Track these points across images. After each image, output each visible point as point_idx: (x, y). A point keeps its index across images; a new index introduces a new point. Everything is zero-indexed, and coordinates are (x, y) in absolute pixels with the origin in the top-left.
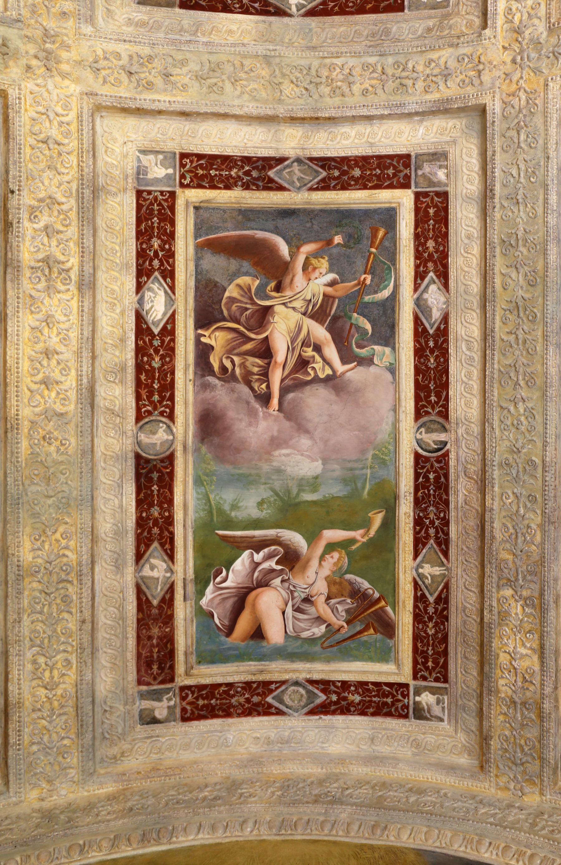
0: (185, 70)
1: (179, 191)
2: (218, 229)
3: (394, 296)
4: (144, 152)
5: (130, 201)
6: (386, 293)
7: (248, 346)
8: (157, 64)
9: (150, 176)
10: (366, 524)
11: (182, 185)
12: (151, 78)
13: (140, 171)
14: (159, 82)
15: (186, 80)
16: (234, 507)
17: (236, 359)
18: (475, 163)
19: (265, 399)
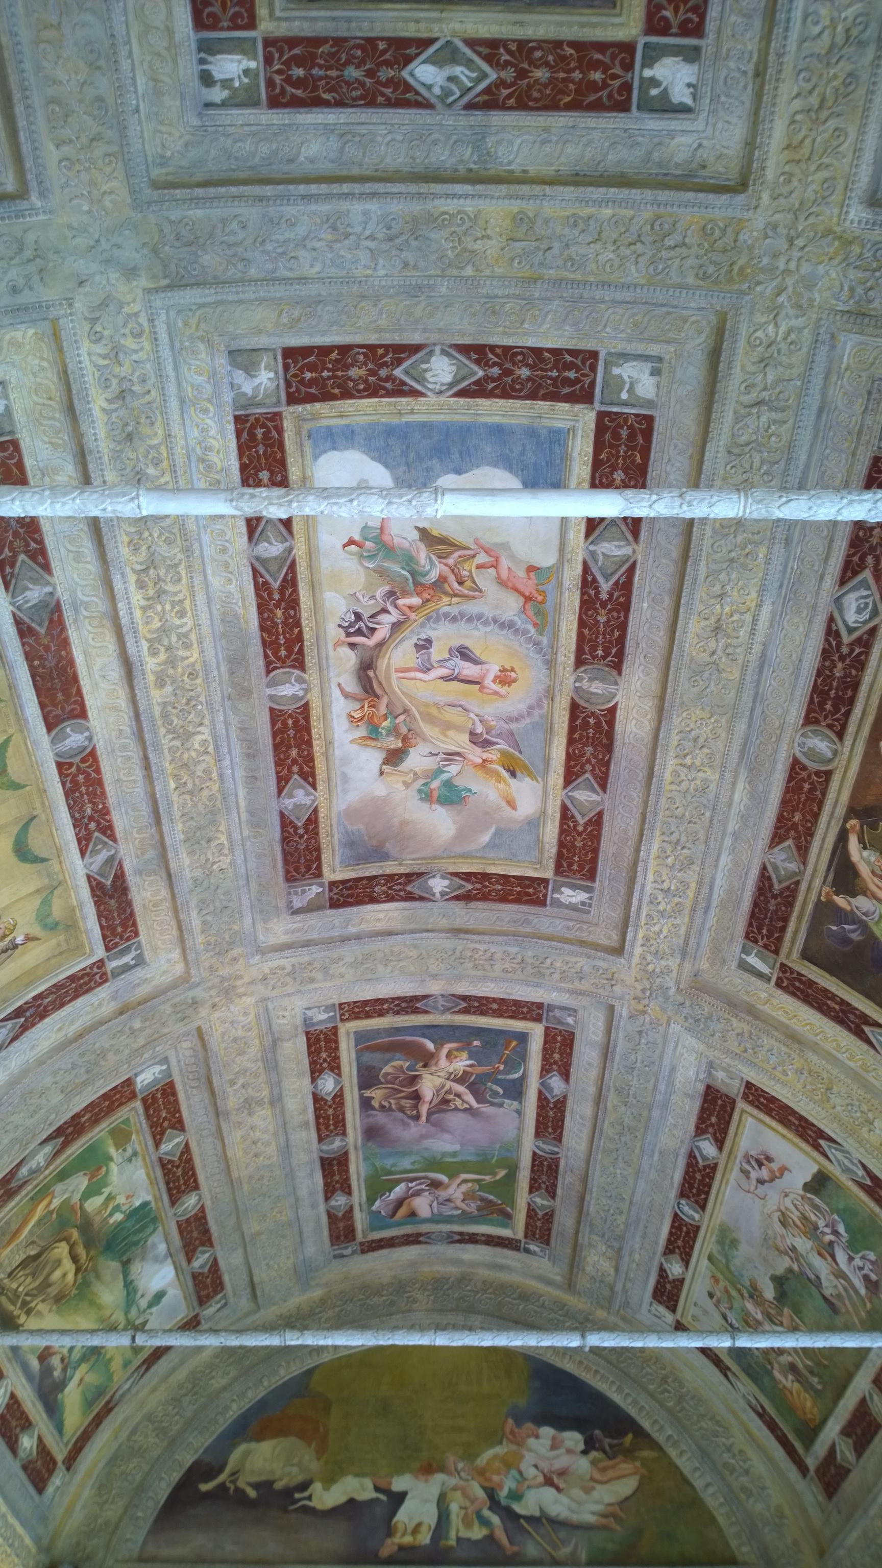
0: (341, 964)
1: (340, 1025)
2: (374, 1039)
3: (523, 1078)
4: (309, 1009)
5: (302, 1041)
6: (516, 1076)
7: (402, 1095)
8: (317, 965)
9: (315, 1020)
10: (494, 1174)
11: (342, 1020)
12: (313, 974)
13: (307, 1021)
14: (319, 976)
15: (343, 970)
16: (392, 1166)
17: (392, 1101)
18: (601, 1025)
19: (417, 1118)
